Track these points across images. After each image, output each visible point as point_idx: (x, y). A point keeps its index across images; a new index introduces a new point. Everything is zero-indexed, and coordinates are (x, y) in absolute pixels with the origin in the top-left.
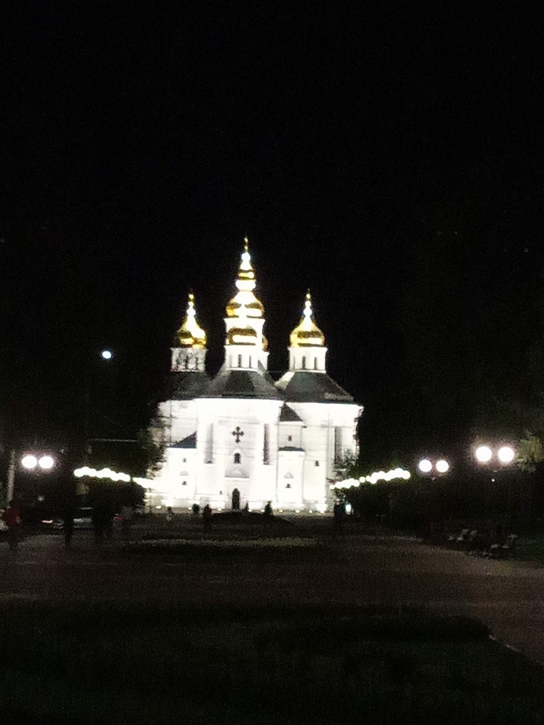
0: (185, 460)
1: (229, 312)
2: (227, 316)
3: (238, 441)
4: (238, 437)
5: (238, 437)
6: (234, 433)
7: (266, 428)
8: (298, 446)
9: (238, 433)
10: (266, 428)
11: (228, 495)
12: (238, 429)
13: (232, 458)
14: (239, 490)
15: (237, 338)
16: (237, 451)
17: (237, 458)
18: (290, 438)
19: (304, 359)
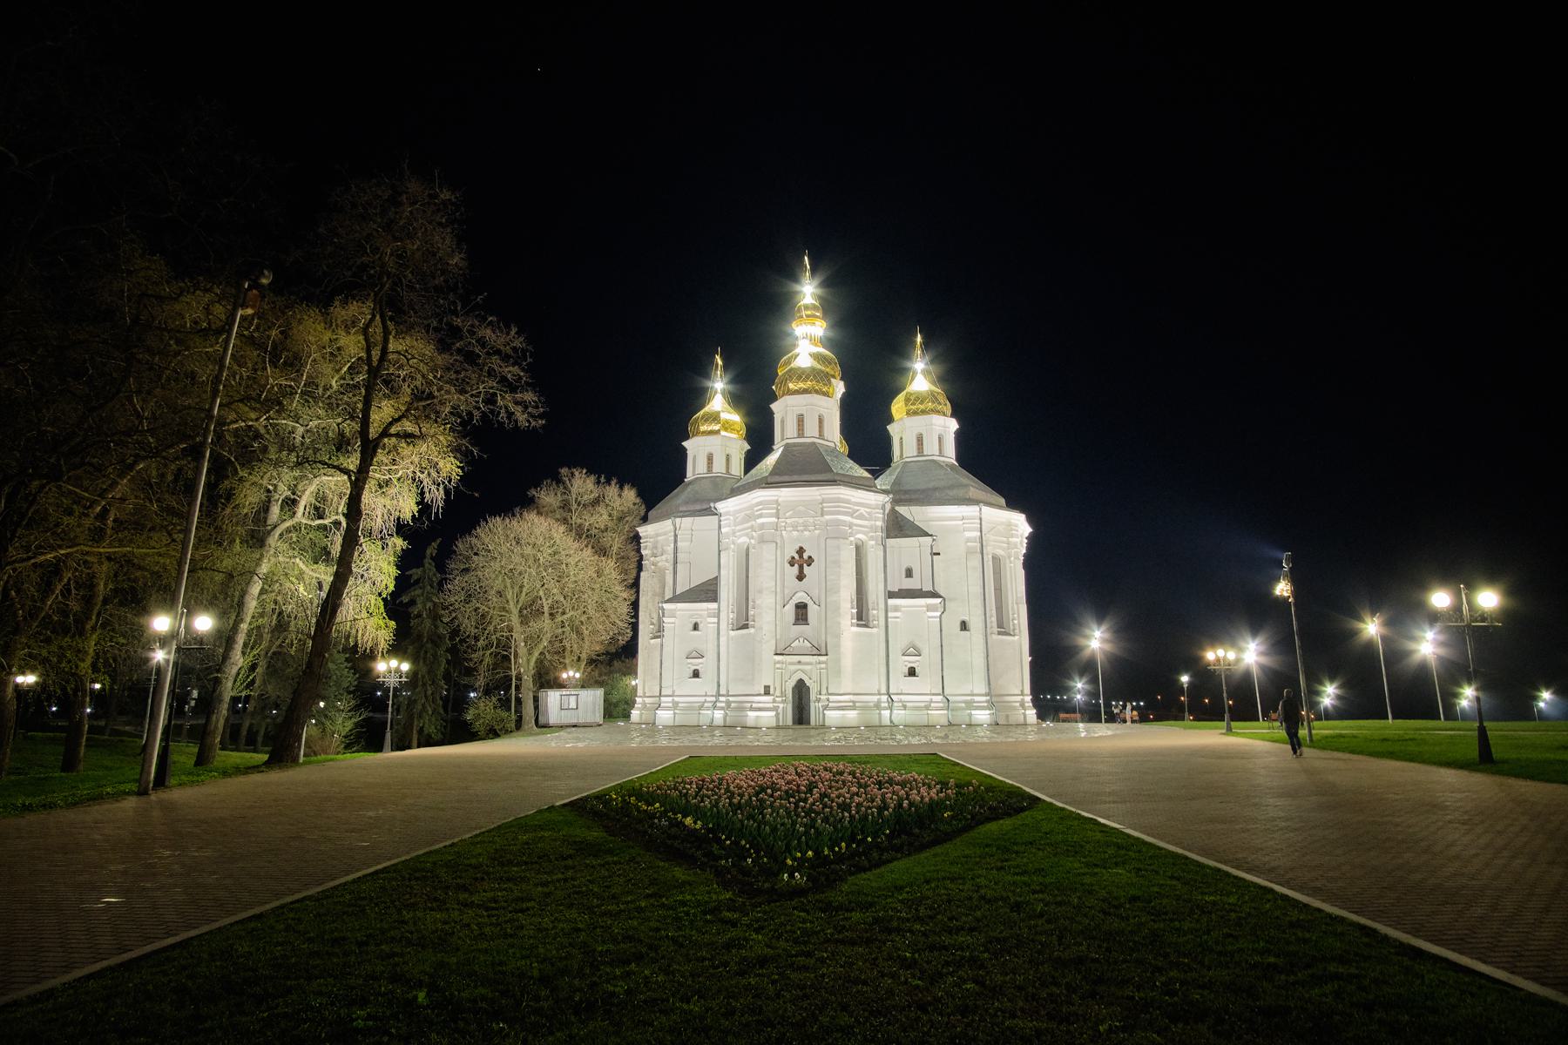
0: (696, 627)
3: (801, 577)
4: (801, 567)
5: (801, 567)
7: (859, 550)
8: (927, 587)
9: (801, 561)
10: (859, 550)
11: (783, 694)
12: (801, 551)
13: (790, 610)
14: (808, 682)
16: (801, 597)
17: (801, 612)
18: (909, 573)
19: (920, 440)
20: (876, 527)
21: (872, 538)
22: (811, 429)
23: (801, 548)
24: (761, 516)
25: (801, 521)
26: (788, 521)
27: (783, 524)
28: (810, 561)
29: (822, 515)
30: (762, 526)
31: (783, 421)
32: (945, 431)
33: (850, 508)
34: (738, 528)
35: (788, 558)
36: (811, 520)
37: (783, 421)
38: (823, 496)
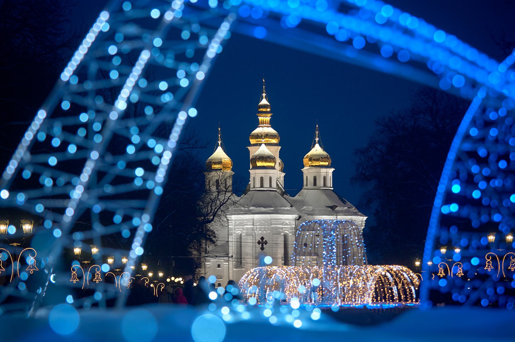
0: (219, 266)
1: (252, 141)
2: (250, 145)
3: (262, 248)
4: (262, 246)
5: (262, 246)
6: (259, 243)
7: (285, 236)
10: (285, 236)
15: (259, 164)
19: (315, 179)
20: (292, 227)
21: (291, 233)
22: (266, 184)
23: (262, 237)
24: (247, 225)
25: (263, 227)
26: (258, 227)
27: (256, 228)
28: (266, 243)
29: (271, 224)
30: (247, 229)
31: (254, 178)
32: (327, 174)
33: (282, 222)
34: (236, 227)
35: (257, 241)
36: (267, 226)
37: (254, 178)
38: (271, 218)
